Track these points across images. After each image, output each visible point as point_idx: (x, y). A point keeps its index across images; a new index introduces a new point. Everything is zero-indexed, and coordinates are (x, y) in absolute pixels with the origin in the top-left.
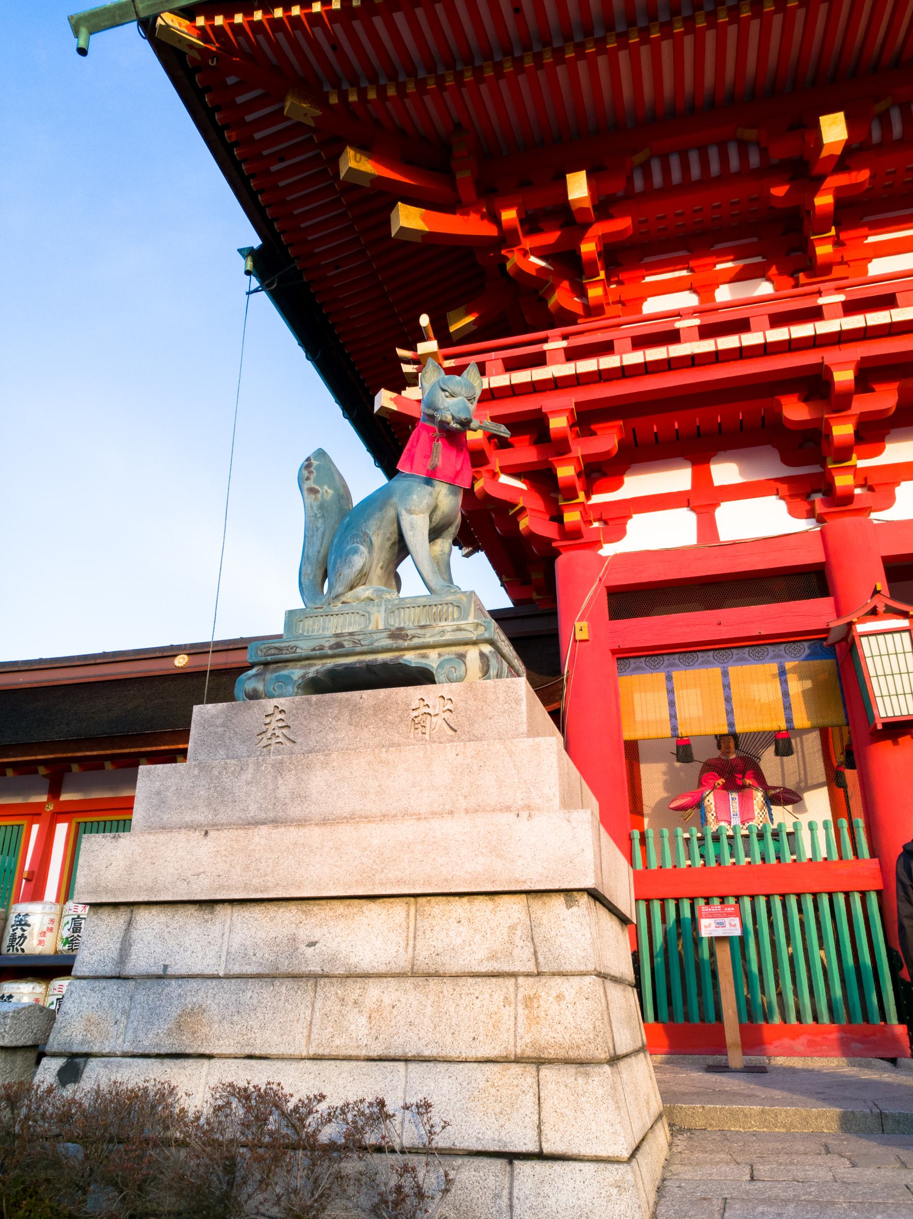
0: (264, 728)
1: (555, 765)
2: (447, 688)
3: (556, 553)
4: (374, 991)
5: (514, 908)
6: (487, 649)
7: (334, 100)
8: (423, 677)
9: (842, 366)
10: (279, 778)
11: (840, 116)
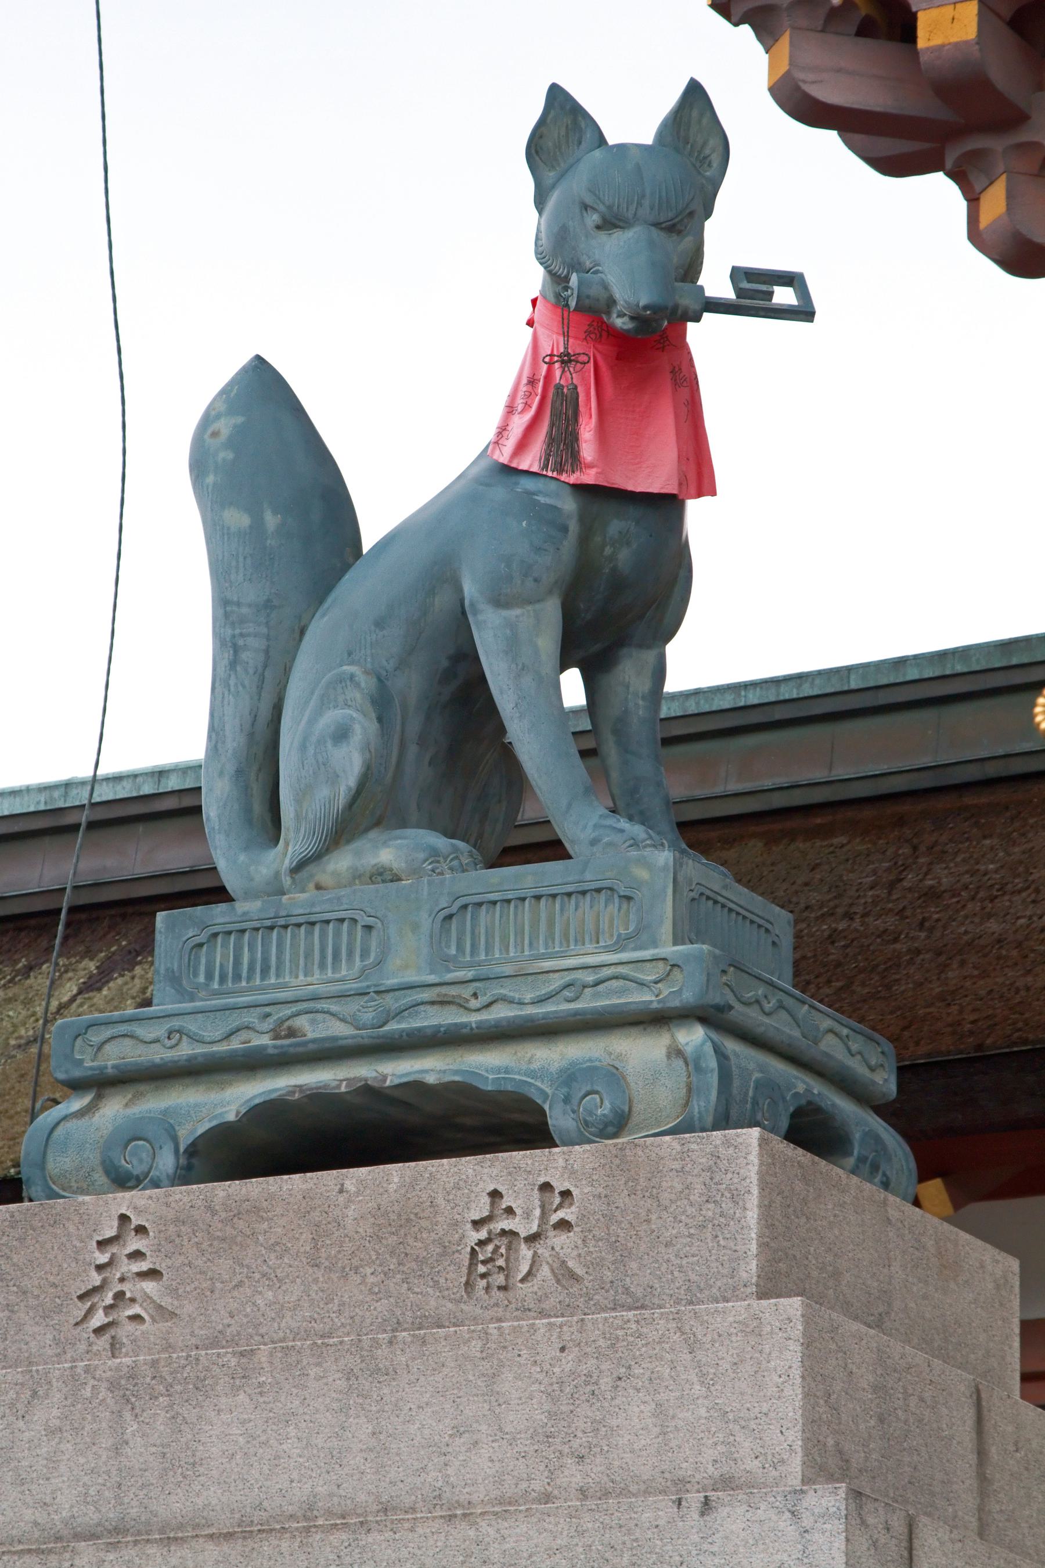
0: (96, 1279)
1: (797, 1372)
2: (561, 1162)
6: (693, 1037)
10: (128, 1415)
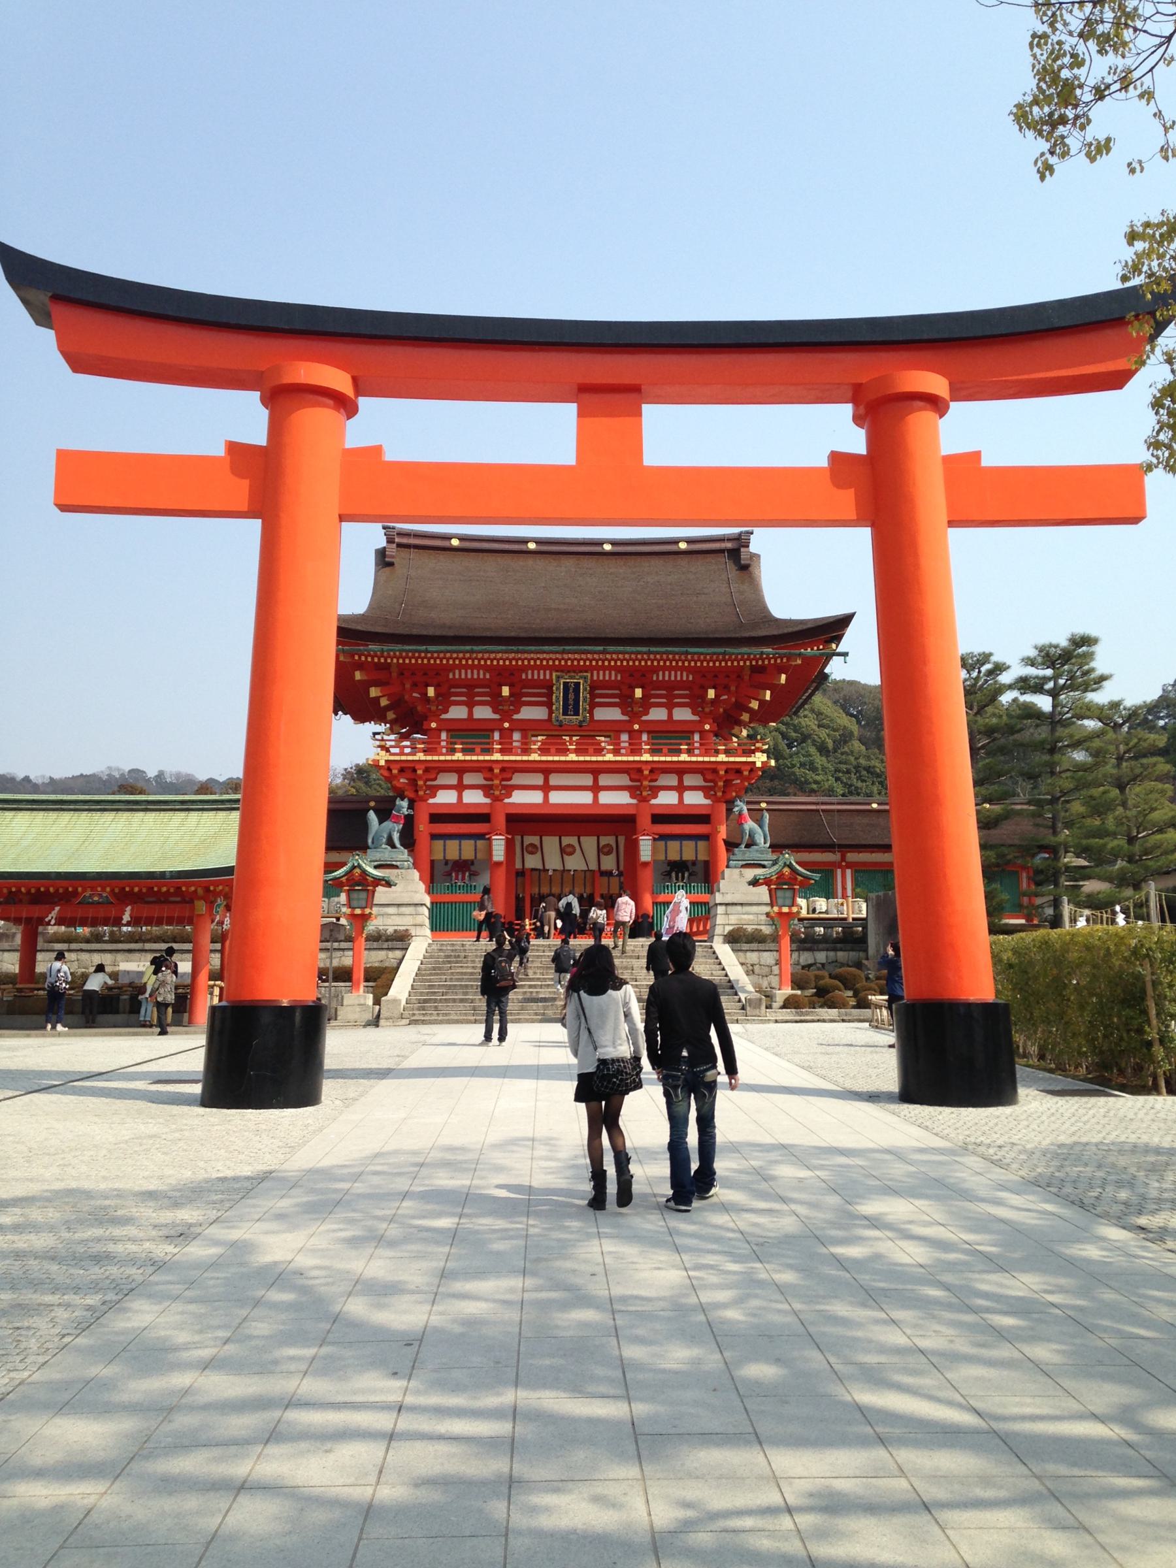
7: (357, 657)
8: (396, 867)
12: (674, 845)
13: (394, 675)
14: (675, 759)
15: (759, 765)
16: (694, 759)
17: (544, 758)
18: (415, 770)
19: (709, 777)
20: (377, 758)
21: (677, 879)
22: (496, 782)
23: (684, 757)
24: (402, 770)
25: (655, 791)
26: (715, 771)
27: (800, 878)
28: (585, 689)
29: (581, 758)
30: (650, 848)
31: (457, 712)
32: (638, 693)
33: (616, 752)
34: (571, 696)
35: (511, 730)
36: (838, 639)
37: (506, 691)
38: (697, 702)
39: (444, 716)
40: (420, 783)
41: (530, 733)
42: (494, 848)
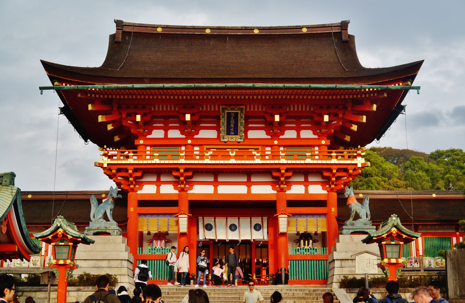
3: (129, 192)
4: (105, 269)
5: (120, 261)
7: (89, 95)
8: (109, 234)
9: (182, 169)
11: (189, 115)
12: (302, 220)
13: (115, 108)
14: (302, 162)
15: (359, 165)
16: (315, 162)
17: (213, 162)
18: (127, 170)
19: (326, 174)
20: (101, 162)
21: (304, 245)
22: (182, 178)
23: (308, 161)
24: (119, 170)
25: (289, 184)
26: (330, 170)
27: (404, 236)
28: (241, 117)
29: (239, 162)
30: (286, 223)
31: (158, 134)
32: (277, 118)
33: (263, 157)
34: (233, 122)
35: (193, 145)
36: (412, 78)
37: (188, 117)
38: (317, 125)
39: (148, 137)
40: (131, 179)
41: (205, 147)
42: (180, 223)
